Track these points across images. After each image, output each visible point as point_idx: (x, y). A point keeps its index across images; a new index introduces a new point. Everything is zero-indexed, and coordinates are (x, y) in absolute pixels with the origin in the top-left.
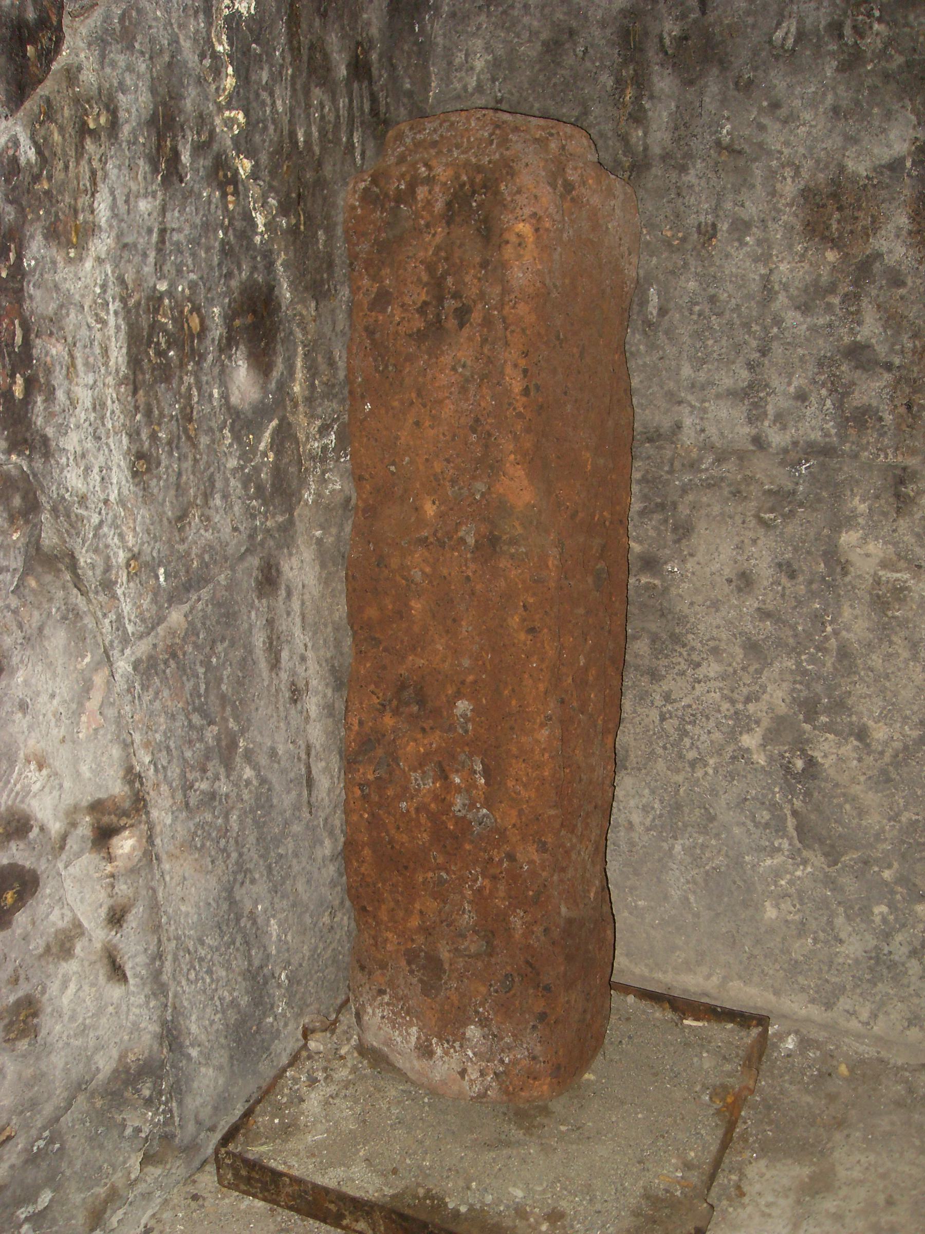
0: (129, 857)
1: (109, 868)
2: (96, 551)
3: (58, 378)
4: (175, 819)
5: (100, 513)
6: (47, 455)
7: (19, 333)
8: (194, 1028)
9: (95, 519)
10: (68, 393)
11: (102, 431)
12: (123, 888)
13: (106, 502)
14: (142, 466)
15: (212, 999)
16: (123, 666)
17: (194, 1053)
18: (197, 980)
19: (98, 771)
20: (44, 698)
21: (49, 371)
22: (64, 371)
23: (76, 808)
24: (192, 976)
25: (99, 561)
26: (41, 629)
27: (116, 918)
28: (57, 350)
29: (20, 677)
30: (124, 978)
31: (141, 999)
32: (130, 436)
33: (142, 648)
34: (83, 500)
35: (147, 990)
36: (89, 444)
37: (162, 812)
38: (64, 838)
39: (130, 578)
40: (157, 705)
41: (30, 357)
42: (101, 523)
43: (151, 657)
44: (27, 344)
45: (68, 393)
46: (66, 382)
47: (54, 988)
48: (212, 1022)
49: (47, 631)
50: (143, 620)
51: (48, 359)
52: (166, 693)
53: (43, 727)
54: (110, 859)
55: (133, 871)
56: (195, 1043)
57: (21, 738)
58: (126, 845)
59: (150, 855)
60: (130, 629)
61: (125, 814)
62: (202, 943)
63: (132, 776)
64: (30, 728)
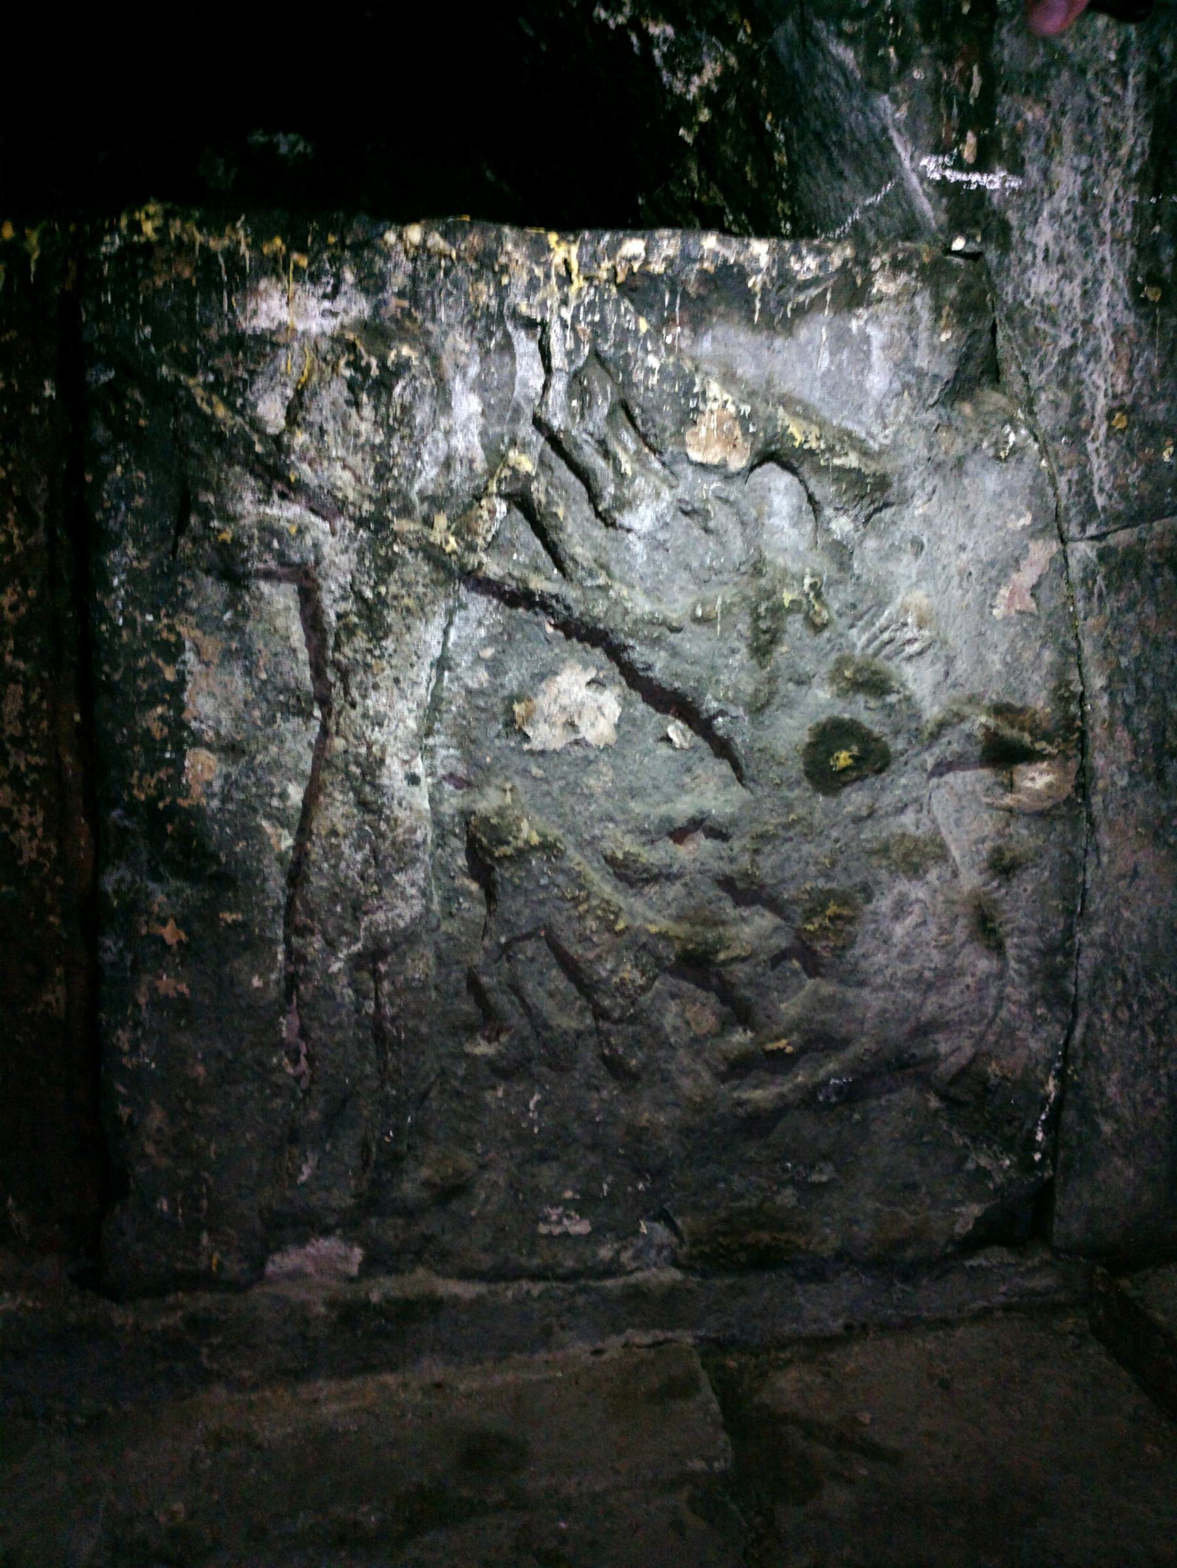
0: (1037, 795)
1: (1008, 800)
2: (1063, 384)
3: (1031, 150)
4: (1134, 786)
5: (1074, 334)
6: (1005, 247)
7: (977, 81)
8: (1111, 1090)
9: (1066, 341)
10: (1045, 173)
11: (1091, 231)
12: (1024, 837)
13: (1087, 323)
14: (1152, 294)
15: (1156, 1069)
16: (1083, 551)
17: (1107, 1128)
18: (1130, 1027)
19: (1012, 668)
20: (948, 546)
21: (1018, 138)
22: (1042, 144)
23: (972, 700)
24: (1124, 1015)
25: (1066, 399)
26: (960, 463)
27: (1003, 867)
28: (1033, 114)
29: (919, 507)
30: (998, 949)
31: (1023, 995)
32: (1139, 249)
33: (1121, 538)
34: (1049, 315)
35: (1036, 988)
36: (1072, 247)
37: (1111, 762)
38: (942, 725)
39: (1111, 433)
40: (1130, 618)
41: (991, 116)
42: (1073, 349)
43: (1129, 550)
44: (988, 97)
45: (1045, 173)
46: (1044, 158)
47: (884, 904)
48: (1148, 1103)
49: (970, 466)
50: (1125, 497)
51: (1019, 124)
52: (1149, 609)
53: (941, 584)
54: (1010, 787)
55: (1043, 816)
56: (1108, 1113)
57: (904, 584)
58: (1037, 779)
59: (1073, 806)
60: (1100, 501)
61: (1048, 737)
62: (1152, 981)
63: (1063, 695)
64: (922, 576)
